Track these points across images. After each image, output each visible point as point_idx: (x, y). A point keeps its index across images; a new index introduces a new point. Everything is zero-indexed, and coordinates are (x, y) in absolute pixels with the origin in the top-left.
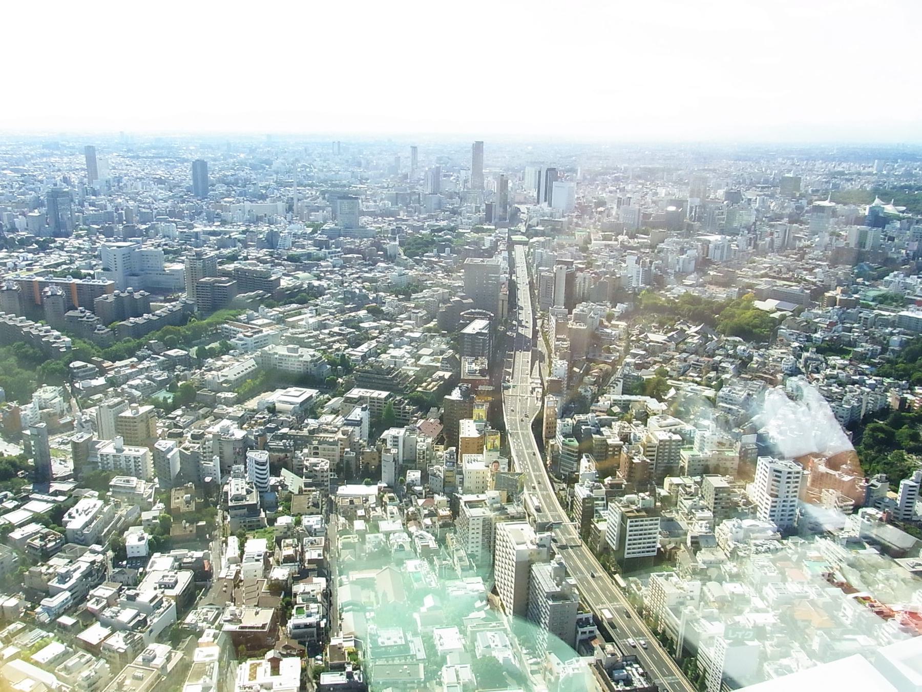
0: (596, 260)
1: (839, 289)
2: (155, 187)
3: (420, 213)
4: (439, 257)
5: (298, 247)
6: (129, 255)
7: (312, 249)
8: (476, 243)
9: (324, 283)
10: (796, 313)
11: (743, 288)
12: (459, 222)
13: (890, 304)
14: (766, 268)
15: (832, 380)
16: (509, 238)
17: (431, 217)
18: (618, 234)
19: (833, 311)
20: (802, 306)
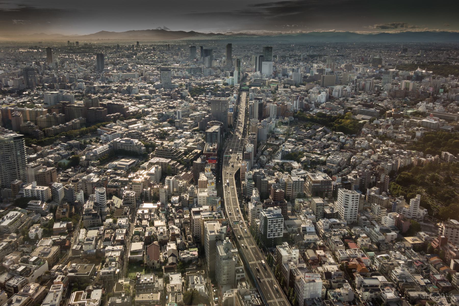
0: (279, 98)
1: (393, 110)
2: (79, 66)
3: (201, 77)
4: (205, 97)
5: (141, 93)
6: (57, 98)
7: (147, 94)
9: (150, 110)
10: (371, 121)
11: (346, 109)
13: (419, 116)
14: (359, 100)
15: (386, 152)
16: (240, 88)
17: (206, 79)
18: (291, 85)
19: (390, 120)
20: (374, 117)
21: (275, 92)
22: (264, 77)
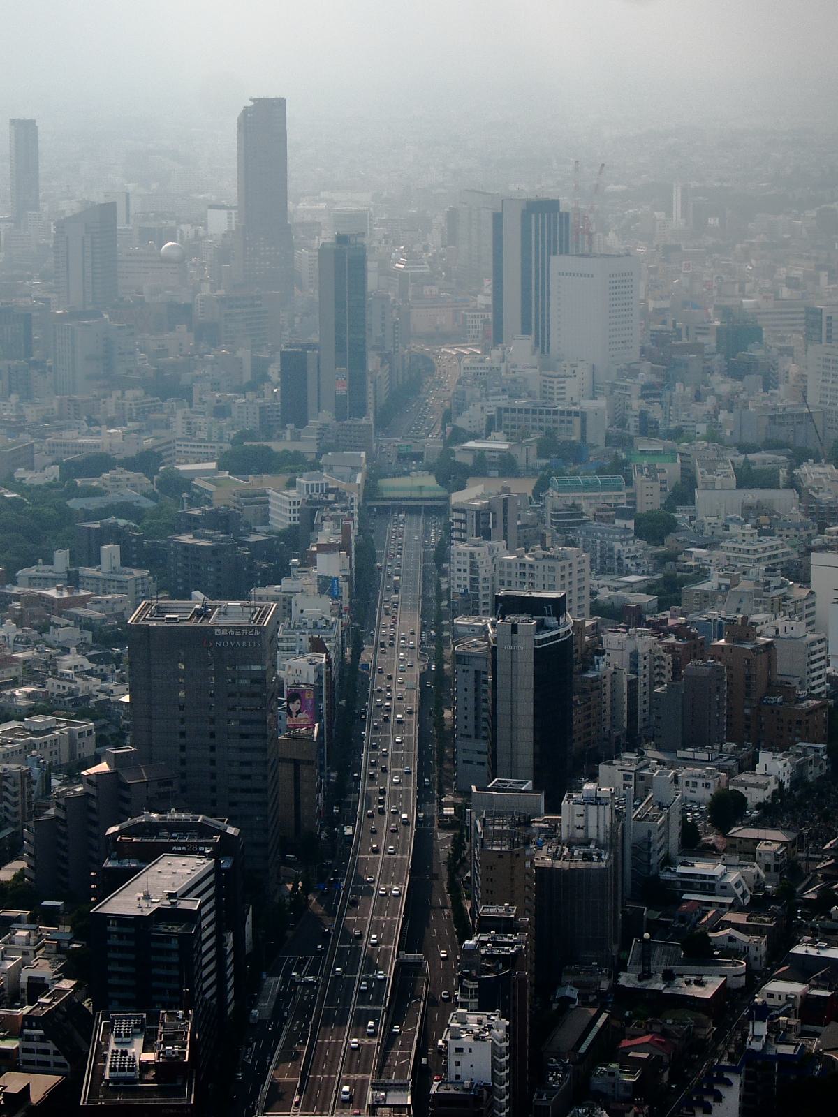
0: (701, 574)
4: (73, 581)
8: (223, 521)
12: (179, 428)
16: (370, 490)
18: (801, 456)
21: (672, 526)
22: (572, 387)
